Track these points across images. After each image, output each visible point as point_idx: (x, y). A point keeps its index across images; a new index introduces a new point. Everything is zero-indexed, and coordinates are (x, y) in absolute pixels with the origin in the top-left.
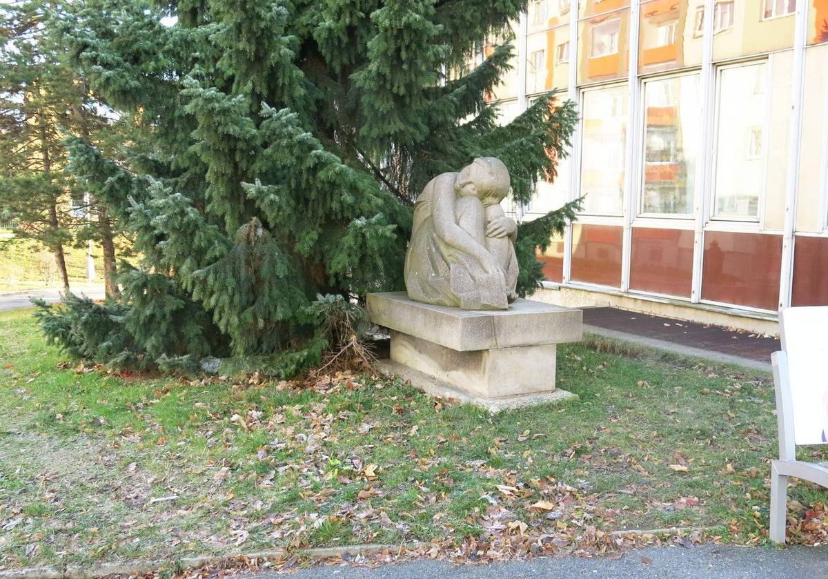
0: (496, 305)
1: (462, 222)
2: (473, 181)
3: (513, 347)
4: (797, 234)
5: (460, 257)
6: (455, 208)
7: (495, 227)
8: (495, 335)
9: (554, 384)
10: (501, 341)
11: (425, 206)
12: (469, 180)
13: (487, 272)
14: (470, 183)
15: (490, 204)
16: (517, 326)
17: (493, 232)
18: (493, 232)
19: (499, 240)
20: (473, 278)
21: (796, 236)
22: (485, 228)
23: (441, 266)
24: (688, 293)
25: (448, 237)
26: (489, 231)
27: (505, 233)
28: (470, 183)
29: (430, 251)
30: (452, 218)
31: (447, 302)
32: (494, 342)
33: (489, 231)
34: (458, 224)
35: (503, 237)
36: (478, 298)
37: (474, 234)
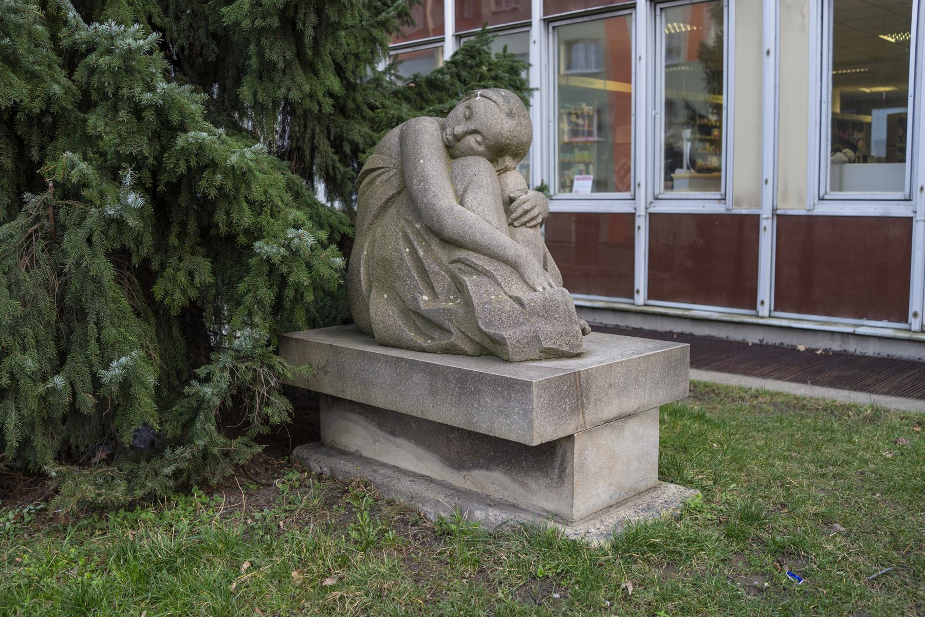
0: (566, 349)
1: (470, 199)
2: (479, 128)
3: (608, 421)
4: (779, 212)
5: (480, 263)
6: (453, 178)
7: (526, 207)
8: (583, 407)
9: (656, 475)
10: (591, 415)
11: (384, 177)
12: (472, 126)
13: (535, 290)
14: (475, 132)
15: (506, 170)
16: (611, 385)
17: (521, 216)
18: (521, 216)
19: (531, 231)
20: (518, 301)
21: (778, 216)
22: (508, 212)
23: (442, 281)
24: (630, 292)
25: (451, 227)
26: (514, 215)
27: (539, 220)
28: (475, 132)
29: (414, 252)
30: (451, 195)
31: (466, 347)
32: (581, 419)
33: (514, 215)
34: (461, 203)
35: (535, 226)
36: (536, 338)
37: (495, 222)
